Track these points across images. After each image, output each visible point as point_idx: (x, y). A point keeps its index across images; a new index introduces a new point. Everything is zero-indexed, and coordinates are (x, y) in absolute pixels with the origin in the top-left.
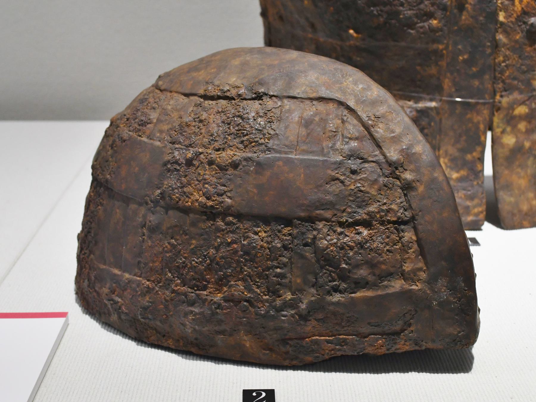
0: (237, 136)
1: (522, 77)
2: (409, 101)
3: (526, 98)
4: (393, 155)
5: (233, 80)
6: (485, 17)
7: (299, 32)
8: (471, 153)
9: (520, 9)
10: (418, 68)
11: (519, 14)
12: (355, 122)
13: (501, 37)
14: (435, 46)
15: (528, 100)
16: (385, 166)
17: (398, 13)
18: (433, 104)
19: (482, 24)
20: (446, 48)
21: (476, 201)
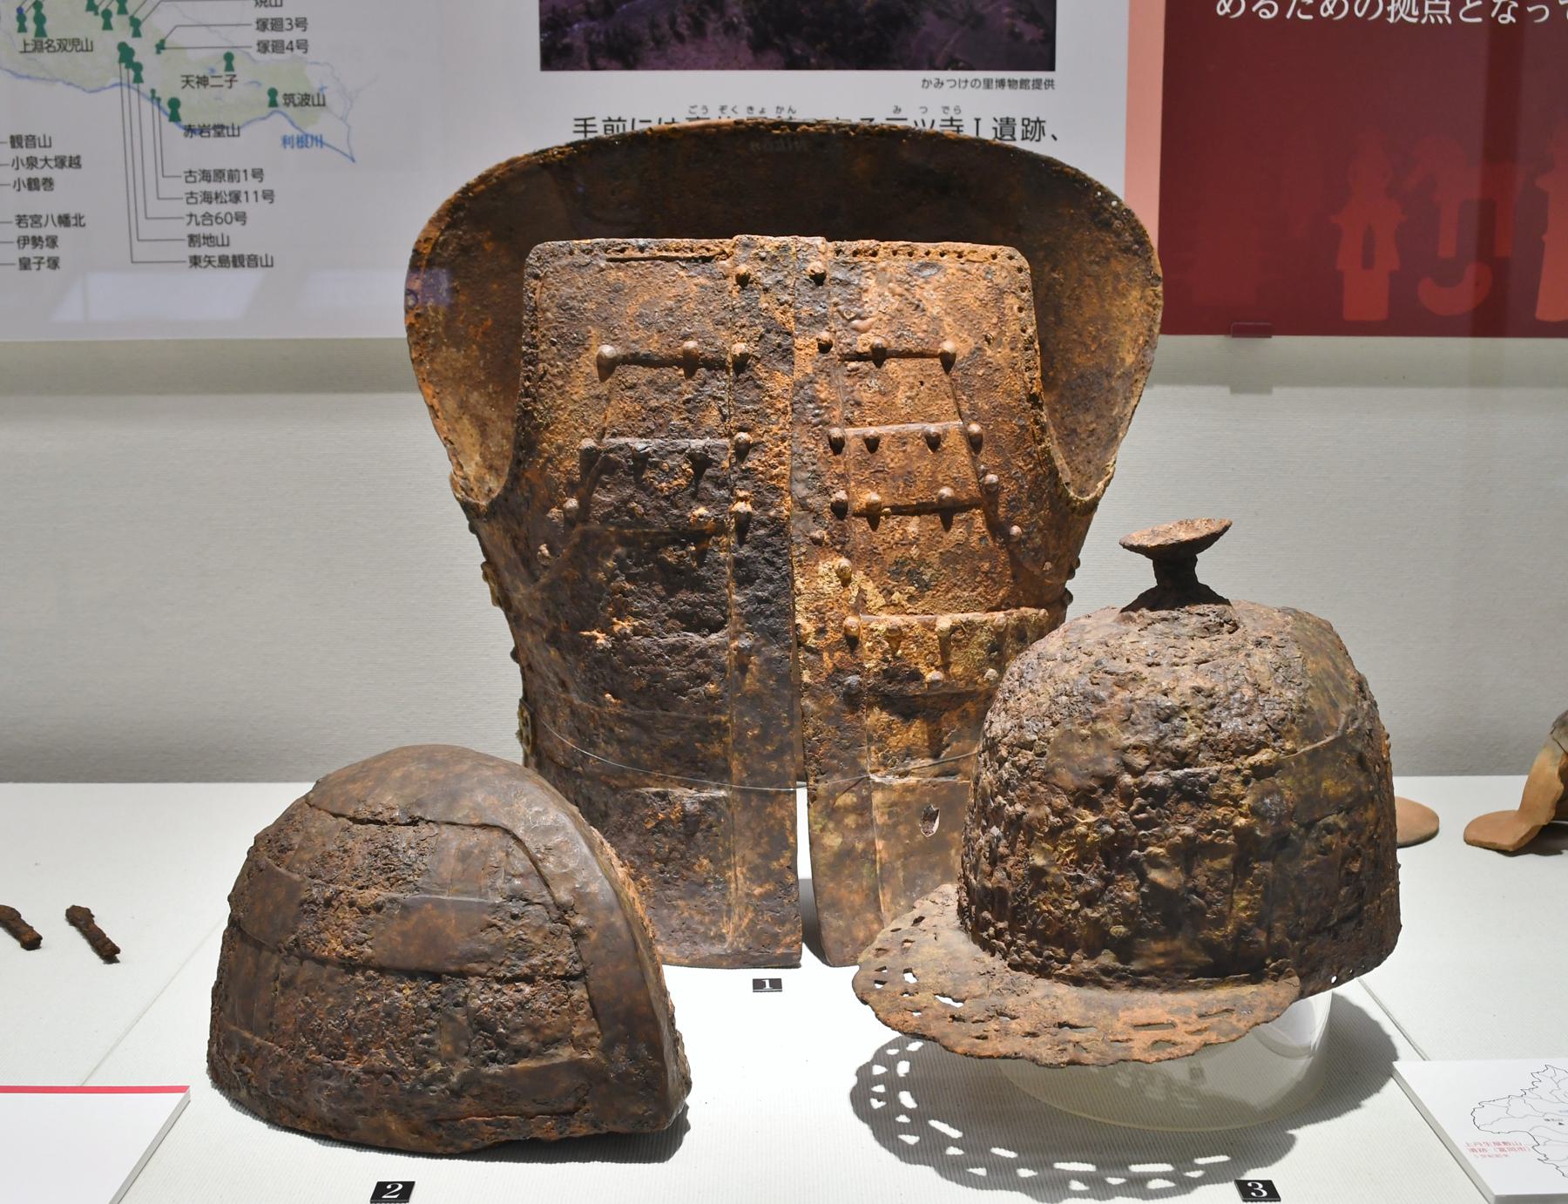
0: (384, 871)
4: (563, 895)
5: (389, 799)
7: (550, 688)
8: (778, 859)
12: (522, 854)
13: (807, 702)
14: (716, 717)
16: (553, 909)
17: (664, 675)
18: (722, 793)
20: (730, 720)
21: (788, 926)
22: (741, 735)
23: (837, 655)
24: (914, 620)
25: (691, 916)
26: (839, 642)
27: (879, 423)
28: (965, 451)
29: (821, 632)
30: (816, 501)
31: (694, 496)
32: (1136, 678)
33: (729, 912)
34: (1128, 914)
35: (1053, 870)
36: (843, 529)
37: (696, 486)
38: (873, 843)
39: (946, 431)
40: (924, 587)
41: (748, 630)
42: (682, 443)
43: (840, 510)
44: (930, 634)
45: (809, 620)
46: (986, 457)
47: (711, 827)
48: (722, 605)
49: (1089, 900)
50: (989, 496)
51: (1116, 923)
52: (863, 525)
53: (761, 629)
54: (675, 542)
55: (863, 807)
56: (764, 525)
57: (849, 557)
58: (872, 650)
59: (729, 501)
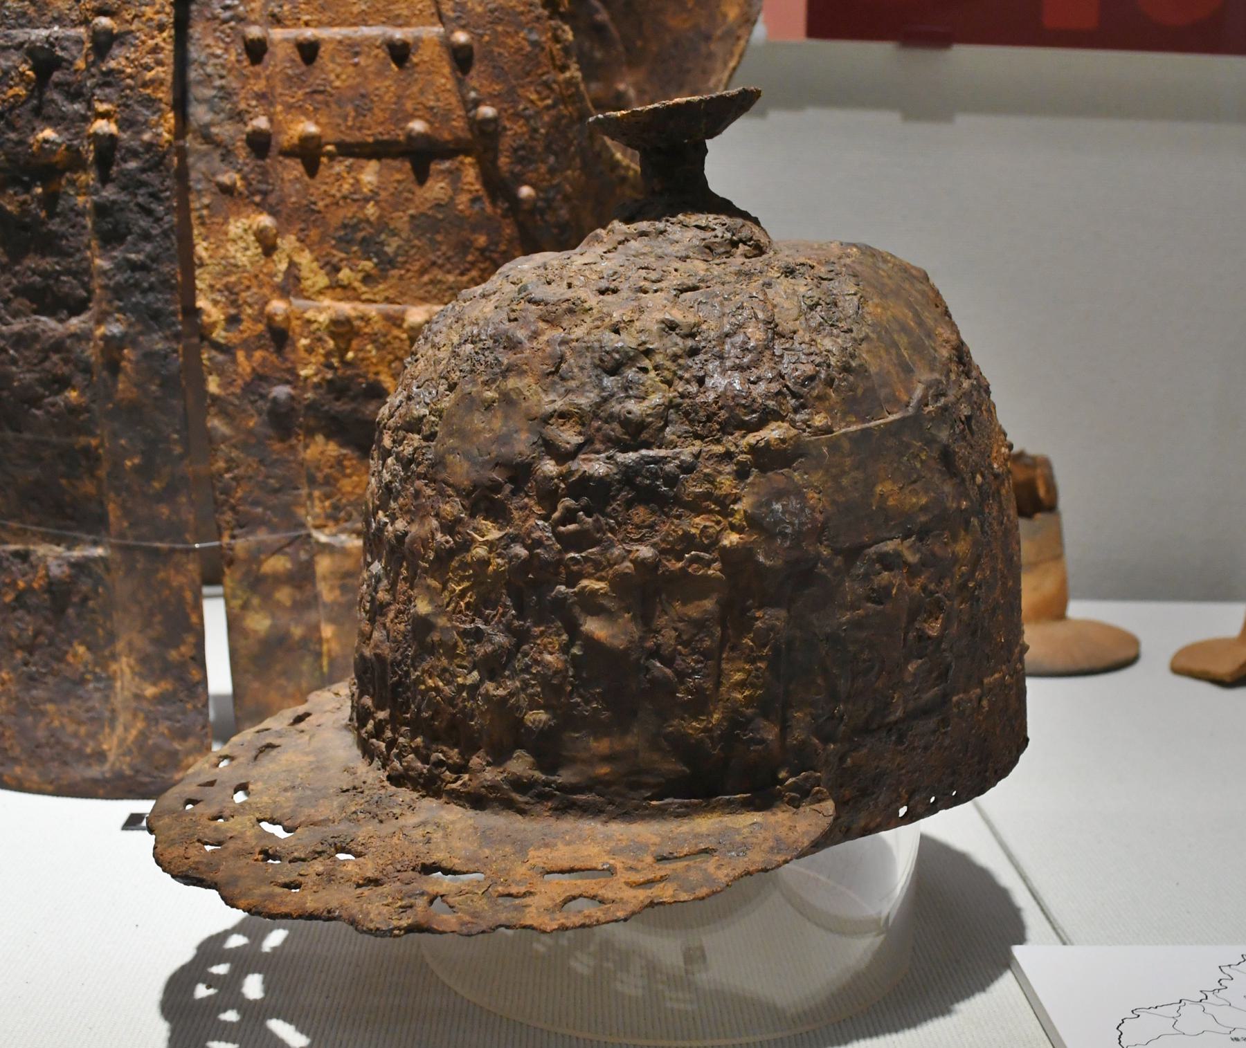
1: (273, 501)
2: (58, 545)
3: (284, 542)
6: (161, 386)
8: (177, 647)
9: (249, 370)
10: (63, 482)
11: (248, 379)
13: (216, 423)
14: (83, 440)
15: (289, 544)
18: (99, 551)
19: (156, 399)
20: (101, 445)
22: (117, 465)
23: (258, 354)
24: (372, 310)
25: (63, 727)
26: (260, 337)
27: (320, 24)
28: (447, 71)
29: (233, 321)
30: (224, 131)
31: (37, 111)
32: (575, 309)
33: (113, 721)
34: (551, 690)
35: (442, 621)
36: (265, 172)
37: (40, 98)
38: (317, 628)
39: (418, 40)
40: (386, 264)
41: (119, 310)
42: (20, 35)
43: (260, 144)
44: (396, 332)
45: (215, 303)
46: (477, 81)
47: (85, 599)
48: (83, 273)
49: (493, 668)
50: (483, 140)
51: (533, 706)
52: (294, 169)
53: (135, 309)
54: (16, 181)
55: (302, 577)
56: (134, 154)
57: (273, 213)
58: (310, 350)
59: (86, 119)
